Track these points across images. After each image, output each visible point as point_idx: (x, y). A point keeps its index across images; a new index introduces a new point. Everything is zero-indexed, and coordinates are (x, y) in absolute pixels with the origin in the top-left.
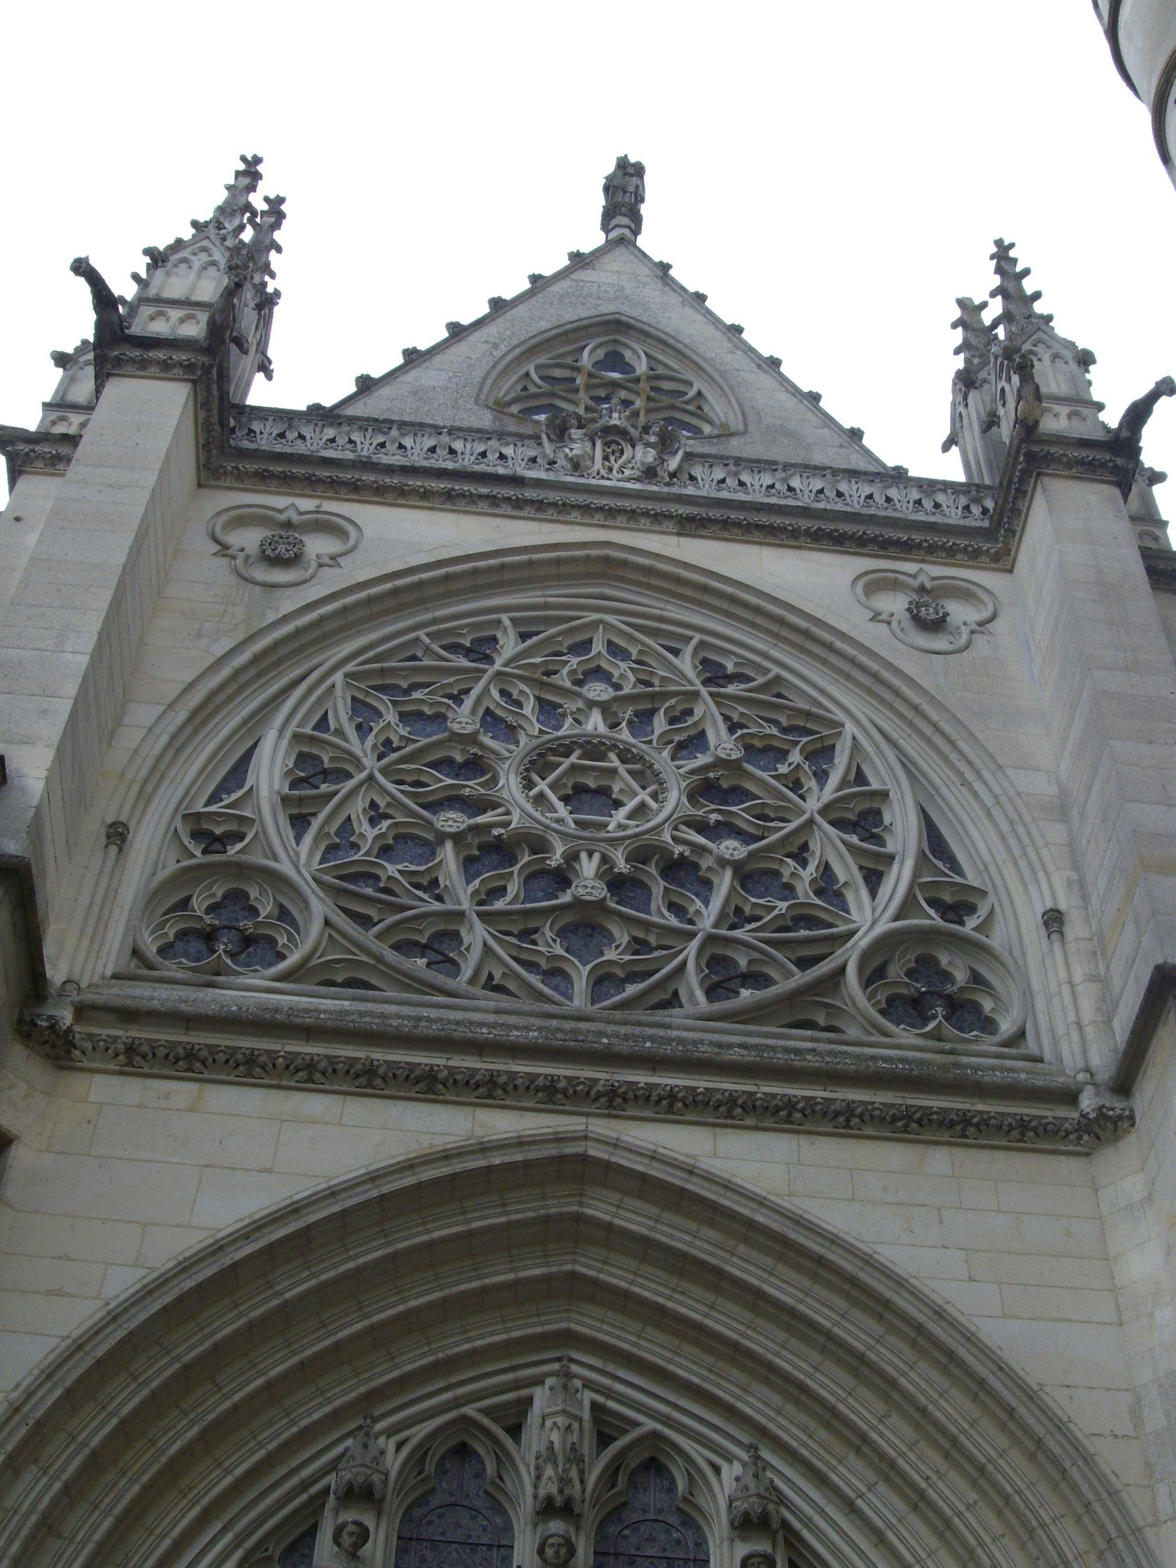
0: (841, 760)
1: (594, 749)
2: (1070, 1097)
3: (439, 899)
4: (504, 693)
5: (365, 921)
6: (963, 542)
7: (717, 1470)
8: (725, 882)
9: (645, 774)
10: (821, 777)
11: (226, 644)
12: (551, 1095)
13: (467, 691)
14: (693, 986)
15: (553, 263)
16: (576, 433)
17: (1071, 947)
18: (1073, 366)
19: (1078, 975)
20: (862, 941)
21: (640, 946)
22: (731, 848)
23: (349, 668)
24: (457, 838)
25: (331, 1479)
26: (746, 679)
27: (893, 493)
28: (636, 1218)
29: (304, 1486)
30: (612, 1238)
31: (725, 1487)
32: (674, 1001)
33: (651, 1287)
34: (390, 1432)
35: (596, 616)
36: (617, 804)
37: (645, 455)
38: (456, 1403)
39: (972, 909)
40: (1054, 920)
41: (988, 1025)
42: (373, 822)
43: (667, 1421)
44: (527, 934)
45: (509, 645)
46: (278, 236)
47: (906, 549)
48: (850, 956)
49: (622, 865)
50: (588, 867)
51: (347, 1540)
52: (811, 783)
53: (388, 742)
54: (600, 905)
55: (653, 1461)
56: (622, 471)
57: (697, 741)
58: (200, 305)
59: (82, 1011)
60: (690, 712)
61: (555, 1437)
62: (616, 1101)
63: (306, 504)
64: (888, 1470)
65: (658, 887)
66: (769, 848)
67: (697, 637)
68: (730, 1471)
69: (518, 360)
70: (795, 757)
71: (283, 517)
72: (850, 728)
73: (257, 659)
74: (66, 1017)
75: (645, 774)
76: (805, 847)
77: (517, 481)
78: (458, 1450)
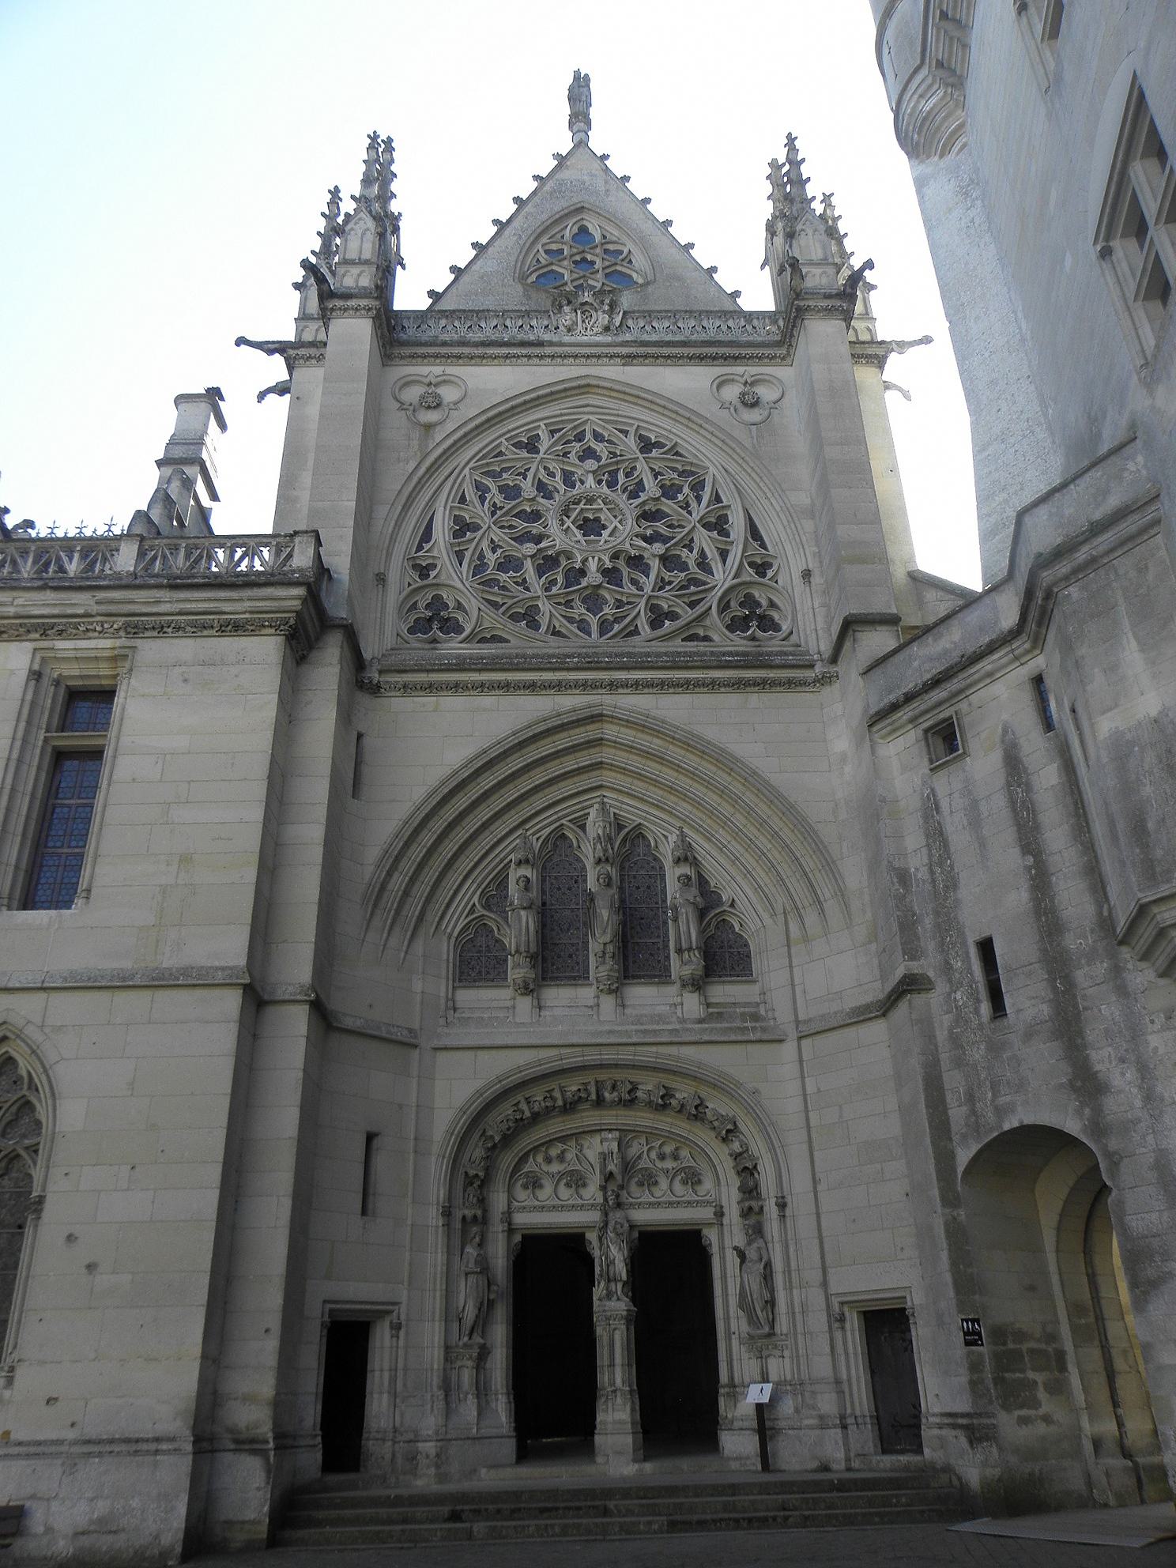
0: (708, 489)
1: (590, 500)
2: (812, 666)
3: (527, 589)
4: (545, 468)
5: (495, 605)
6: (767, 351)
7: (666, 837)
8: (655, 565)
9: (615, 510)
10: (699, 499)
11: (412, 465)
12: (585, 686)
13: (528, 470)
15: (546, 167)
16: (567, 309)
17: (814, 587)
18: (824, 237)
19: (816, 605)
20: (718, 593)
21: (619, 604)
22: (659, 548)
23: (471, 465)
24: (532, 557)
25: (512, 856)
26: (663, 446)
27: (731, 323)
28: (627, 735)
29: (502, 861)
30: (616, 744)
32: (635, 632)
33: (635, 762)
34: (534, 834)
35: (586, 417)
36: (604, 527)
37: (603, 319)
38: (559, 819)
39: (770, 565)
40: (807, 574)
41: (776, 628)
42: (494, 551)
43: (645, 819)
44: (568, 604)
45: (545, 443)
46: (393, 168)
47: (736, 359)
48: (713, 599)
49: (608, 565)
50: (593, 565)
51: (522, 884)
52: (694, 504)
53: (495, 505)
54: (599, 586)
56: (590, 331)
57: (640, 486)
58: (367, 262)
59: (381, 672)
60: (634, 468)
61: (600, 832)
62: (613, 686)
63: (437, 370)
64: (737, 834)
65: (625, 571)
66: (675, 544)
67: (637, 423)
68: (673, 838)
69: (533, 243)
70: (686, 490)
71: (427, 381)
72: (712, 470)
73: (428, 470)
74: (376, 677)
75: (615, 510)
76: (692, 540)
77: (540, 344)
78: (559, 837)
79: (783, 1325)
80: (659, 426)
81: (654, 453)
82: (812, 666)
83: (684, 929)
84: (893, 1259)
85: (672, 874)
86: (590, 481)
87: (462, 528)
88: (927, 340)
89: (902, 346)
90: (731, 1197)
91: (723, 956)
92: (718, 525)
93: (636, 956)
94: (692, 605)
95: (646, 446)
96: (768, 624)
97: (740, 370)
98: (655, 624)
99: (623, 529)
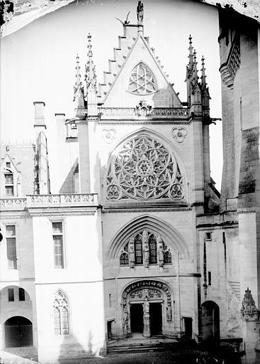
14: (155, 194)
31: (158, 239)
40: (188, 184)
55: (152, 235)
62: (149, 211)
78: (138, 235)
79: (173, 319)
80: (159, 140)
81: (158, 148)
82: (186, 206)
83: (160, 257)
84: (193, 314)
85: (159, 245)
86: (144, 156)
87: (118, 168)
88: (221, 120)
89: (215, 119)
90: (165, 299)
91: (167, 259)
92: (170, 167)
93: (152, 261)
94: (165, 188)
95: (157, 145)
96: (179, 193)
97: (178, 126)
98: (157, 193)
99: (151, 170)
